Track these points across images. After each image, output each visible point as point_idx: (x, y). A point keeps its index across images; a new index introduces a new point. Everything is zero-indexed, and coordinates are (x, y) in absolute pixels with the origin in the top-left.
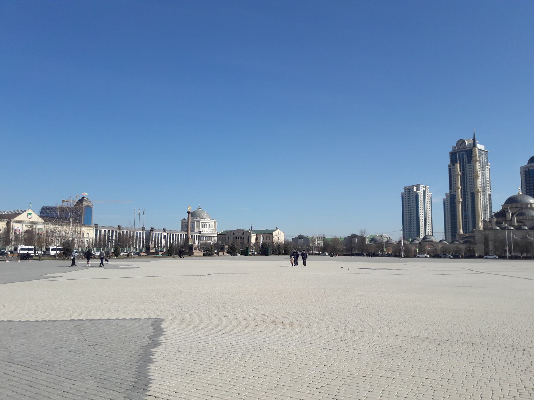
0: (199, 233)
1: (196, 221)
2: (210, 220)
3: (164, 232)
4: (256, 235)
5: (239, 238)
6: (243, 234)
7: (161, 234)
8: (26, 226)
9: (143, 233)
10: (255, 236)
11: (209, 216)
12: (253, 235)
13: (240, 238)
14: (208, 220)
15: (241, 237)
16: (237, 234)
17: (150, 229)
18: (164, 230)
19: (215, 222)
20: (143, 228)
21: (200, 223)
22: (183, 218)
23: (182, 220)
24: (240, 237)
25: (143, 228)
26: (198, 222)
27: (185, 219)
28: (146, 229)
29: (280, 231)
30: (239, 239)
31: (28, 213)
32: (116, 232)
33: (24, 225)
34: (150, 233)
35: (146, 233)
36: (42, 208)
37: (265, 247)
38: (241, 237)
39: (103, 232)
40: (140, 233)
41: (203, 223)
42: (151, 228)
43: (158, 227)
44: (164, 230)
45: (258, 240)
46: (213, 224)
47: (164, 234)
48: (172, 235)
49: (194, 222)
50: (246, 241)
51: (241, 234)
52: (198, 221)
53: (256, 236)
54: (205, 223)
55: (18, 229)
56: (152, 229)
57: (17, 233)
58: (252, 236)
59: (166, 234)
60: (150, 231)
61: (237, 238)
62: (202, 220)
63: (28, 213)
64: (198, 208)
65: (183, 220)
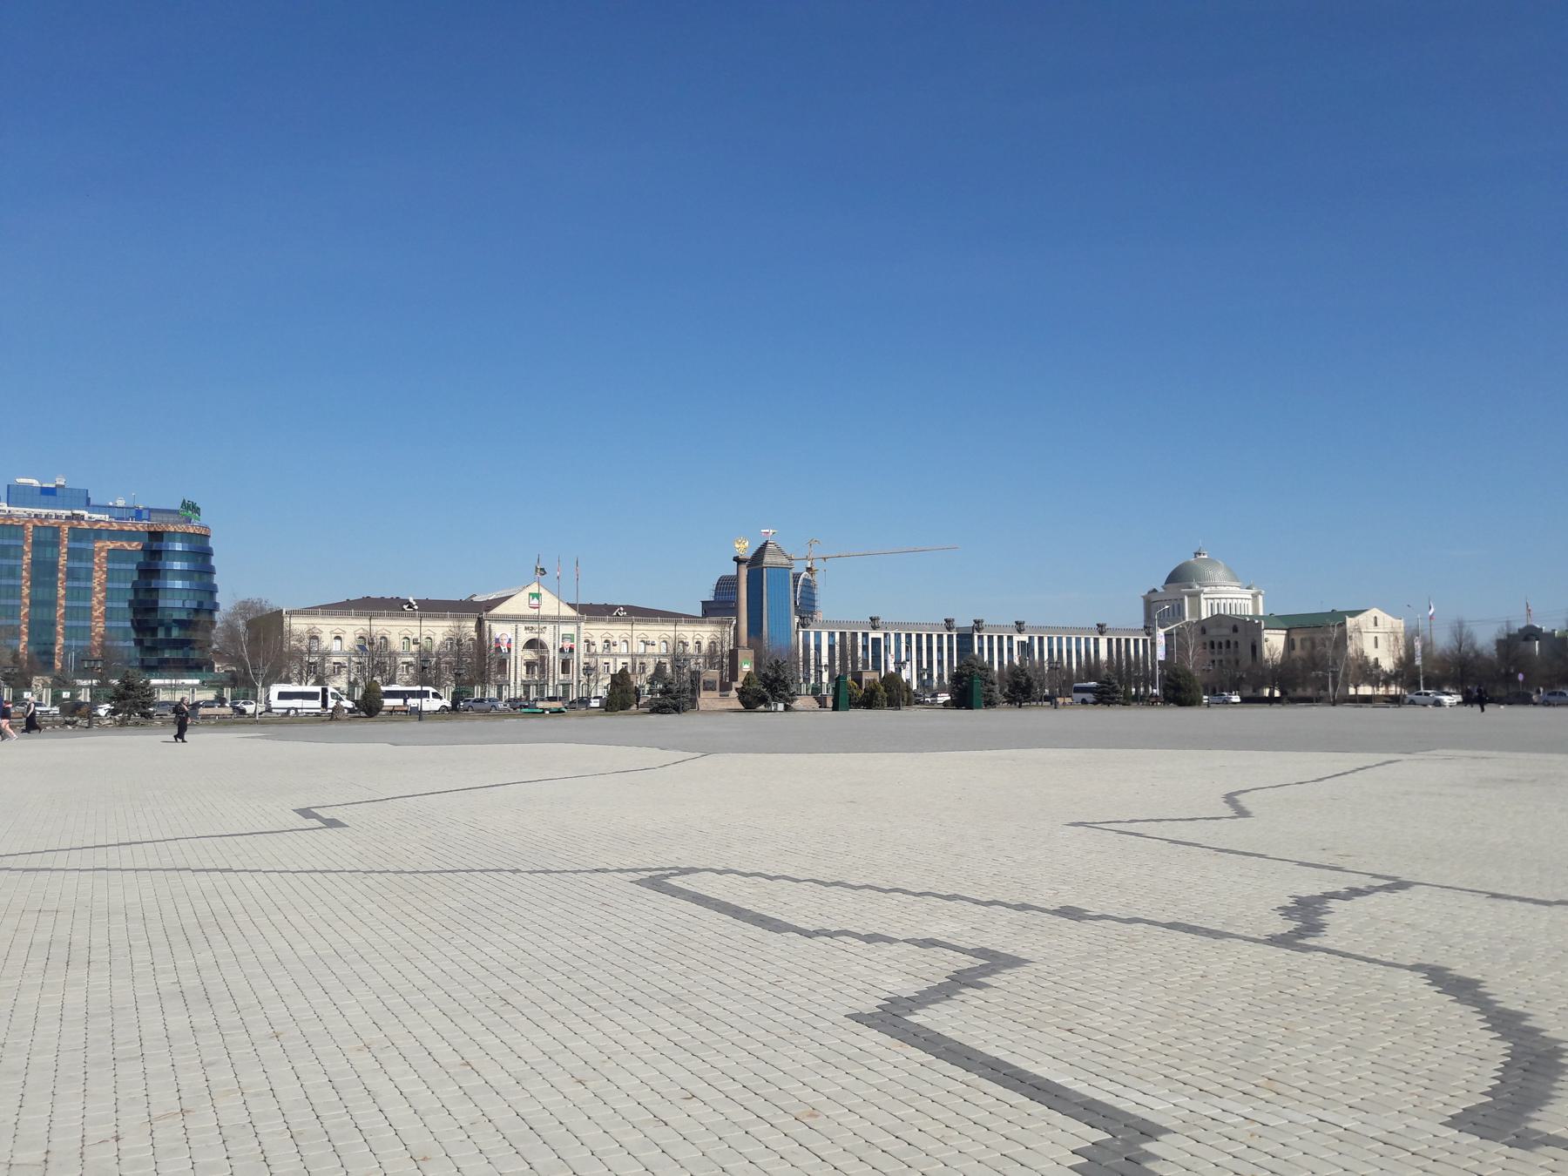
0: (1144, 632)
1: (1189, 596)
2: (1238, 589)
3: (1101, 633)
4: (1285, 632)
5: (1220, 644)
6: (1235, 629)
7: (1010, 638)
8: (526, 628)
9: (950, 637)
10: (1284, 637)
11: (1234, 577)
12: (1268, 631)
13: (1224, 647)
14: (1231, 588)
15: (1228, 643)
16: (1213, 632)
17: (972, 624)
18: (1101, 629)
19: (1255, 596)
20: (949, 624)
21: (1203, 603)
22: (1151, 589)
23: (1145, 593)
24: (1232, 642)
25: (949, 624)
26: (1197, 598)
27: (1155, 591)
28: (957, 624)
29: (1381, 615)
30: (1213, 647)
31: (530, 594)
32: (865, 635)
33: (521, 626)
34: (971, 636)
35: (957, 635)
36: (720, 580)
37: (966, 676)
38: (1228, 643)
39: (825, 636)
40: (940, 637)
41: (1212, 601)
42: (975, 621)
43: (997, 617)
44: (1020, 627)
45: (1294, 648)
46: (1250, 602)
47: (1017, 638)
48: (995, 639)
49: (1183, 600)
50: (1245, 650)
51: (1227, 631)
52: (1195, 596)
53: (1288, 635)
54: (1218, 601)
55: (504, 637)
56: (978, 626)
57: (502, 648)
58: (1266, 636)
59: (1025, 638)
60: (973, 632)
61: (1216, 646)
62: (1206, 590)
63: (530, 594)
64: (1196, 554)
65: (1149, 593)
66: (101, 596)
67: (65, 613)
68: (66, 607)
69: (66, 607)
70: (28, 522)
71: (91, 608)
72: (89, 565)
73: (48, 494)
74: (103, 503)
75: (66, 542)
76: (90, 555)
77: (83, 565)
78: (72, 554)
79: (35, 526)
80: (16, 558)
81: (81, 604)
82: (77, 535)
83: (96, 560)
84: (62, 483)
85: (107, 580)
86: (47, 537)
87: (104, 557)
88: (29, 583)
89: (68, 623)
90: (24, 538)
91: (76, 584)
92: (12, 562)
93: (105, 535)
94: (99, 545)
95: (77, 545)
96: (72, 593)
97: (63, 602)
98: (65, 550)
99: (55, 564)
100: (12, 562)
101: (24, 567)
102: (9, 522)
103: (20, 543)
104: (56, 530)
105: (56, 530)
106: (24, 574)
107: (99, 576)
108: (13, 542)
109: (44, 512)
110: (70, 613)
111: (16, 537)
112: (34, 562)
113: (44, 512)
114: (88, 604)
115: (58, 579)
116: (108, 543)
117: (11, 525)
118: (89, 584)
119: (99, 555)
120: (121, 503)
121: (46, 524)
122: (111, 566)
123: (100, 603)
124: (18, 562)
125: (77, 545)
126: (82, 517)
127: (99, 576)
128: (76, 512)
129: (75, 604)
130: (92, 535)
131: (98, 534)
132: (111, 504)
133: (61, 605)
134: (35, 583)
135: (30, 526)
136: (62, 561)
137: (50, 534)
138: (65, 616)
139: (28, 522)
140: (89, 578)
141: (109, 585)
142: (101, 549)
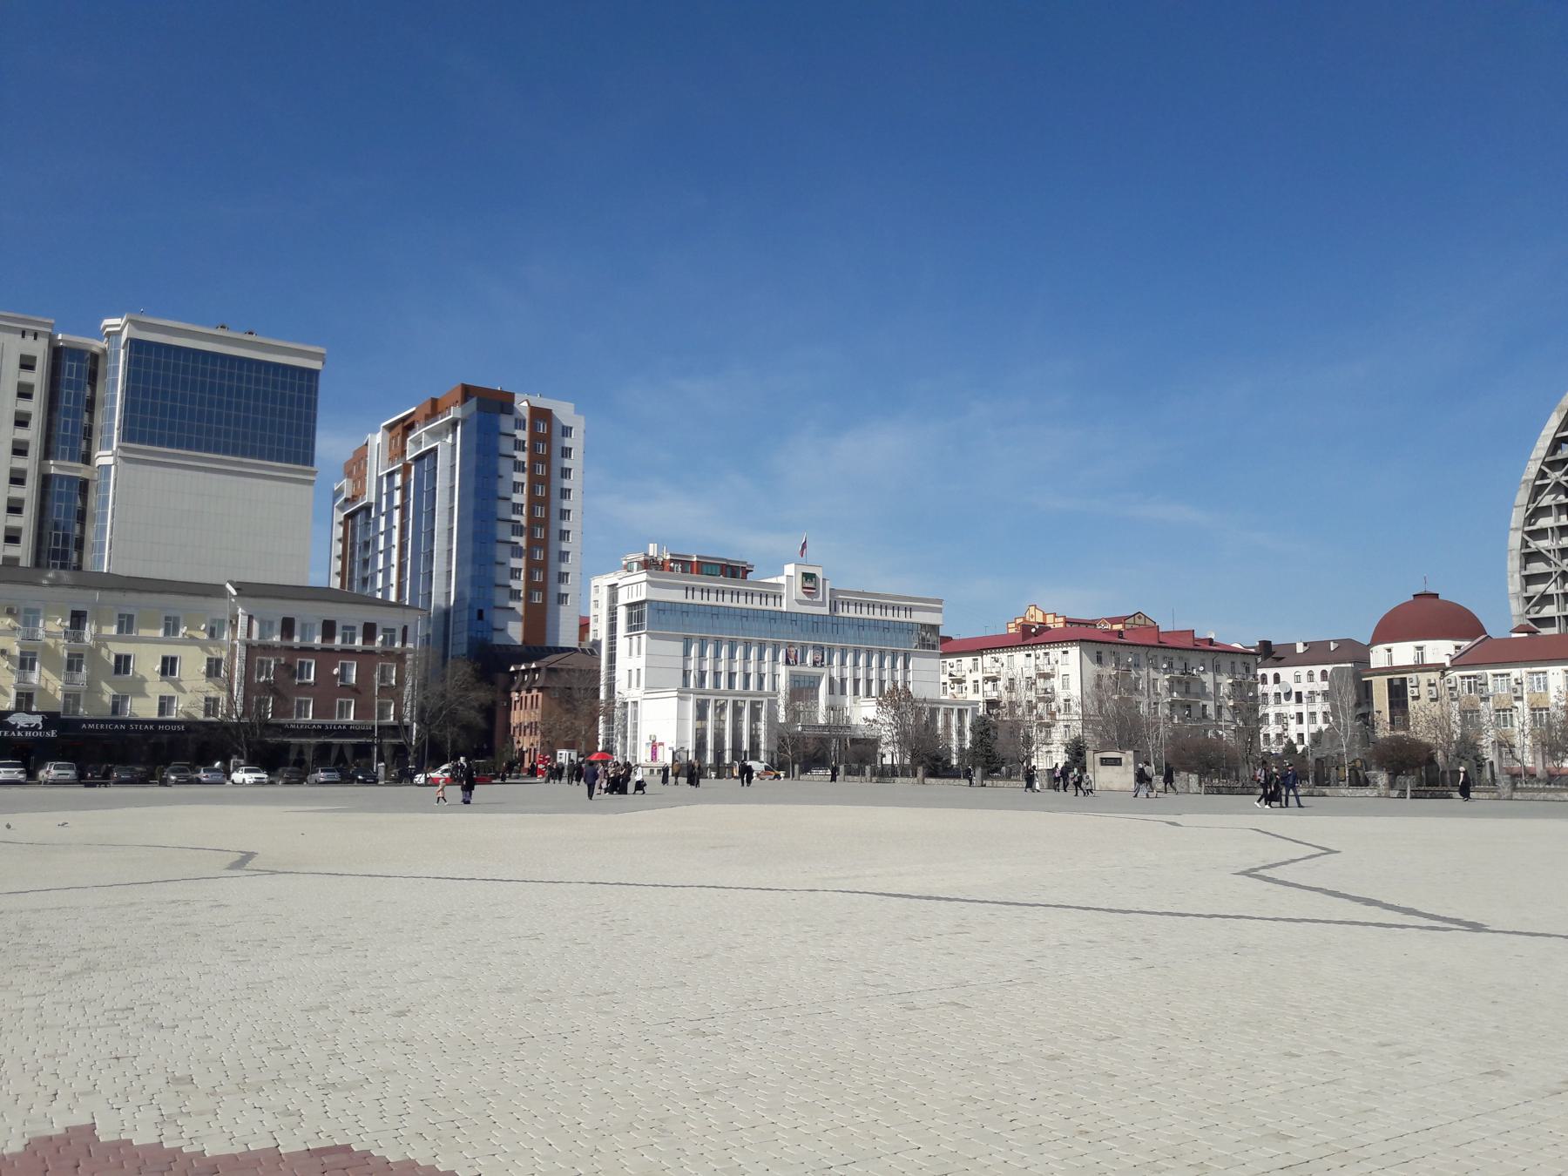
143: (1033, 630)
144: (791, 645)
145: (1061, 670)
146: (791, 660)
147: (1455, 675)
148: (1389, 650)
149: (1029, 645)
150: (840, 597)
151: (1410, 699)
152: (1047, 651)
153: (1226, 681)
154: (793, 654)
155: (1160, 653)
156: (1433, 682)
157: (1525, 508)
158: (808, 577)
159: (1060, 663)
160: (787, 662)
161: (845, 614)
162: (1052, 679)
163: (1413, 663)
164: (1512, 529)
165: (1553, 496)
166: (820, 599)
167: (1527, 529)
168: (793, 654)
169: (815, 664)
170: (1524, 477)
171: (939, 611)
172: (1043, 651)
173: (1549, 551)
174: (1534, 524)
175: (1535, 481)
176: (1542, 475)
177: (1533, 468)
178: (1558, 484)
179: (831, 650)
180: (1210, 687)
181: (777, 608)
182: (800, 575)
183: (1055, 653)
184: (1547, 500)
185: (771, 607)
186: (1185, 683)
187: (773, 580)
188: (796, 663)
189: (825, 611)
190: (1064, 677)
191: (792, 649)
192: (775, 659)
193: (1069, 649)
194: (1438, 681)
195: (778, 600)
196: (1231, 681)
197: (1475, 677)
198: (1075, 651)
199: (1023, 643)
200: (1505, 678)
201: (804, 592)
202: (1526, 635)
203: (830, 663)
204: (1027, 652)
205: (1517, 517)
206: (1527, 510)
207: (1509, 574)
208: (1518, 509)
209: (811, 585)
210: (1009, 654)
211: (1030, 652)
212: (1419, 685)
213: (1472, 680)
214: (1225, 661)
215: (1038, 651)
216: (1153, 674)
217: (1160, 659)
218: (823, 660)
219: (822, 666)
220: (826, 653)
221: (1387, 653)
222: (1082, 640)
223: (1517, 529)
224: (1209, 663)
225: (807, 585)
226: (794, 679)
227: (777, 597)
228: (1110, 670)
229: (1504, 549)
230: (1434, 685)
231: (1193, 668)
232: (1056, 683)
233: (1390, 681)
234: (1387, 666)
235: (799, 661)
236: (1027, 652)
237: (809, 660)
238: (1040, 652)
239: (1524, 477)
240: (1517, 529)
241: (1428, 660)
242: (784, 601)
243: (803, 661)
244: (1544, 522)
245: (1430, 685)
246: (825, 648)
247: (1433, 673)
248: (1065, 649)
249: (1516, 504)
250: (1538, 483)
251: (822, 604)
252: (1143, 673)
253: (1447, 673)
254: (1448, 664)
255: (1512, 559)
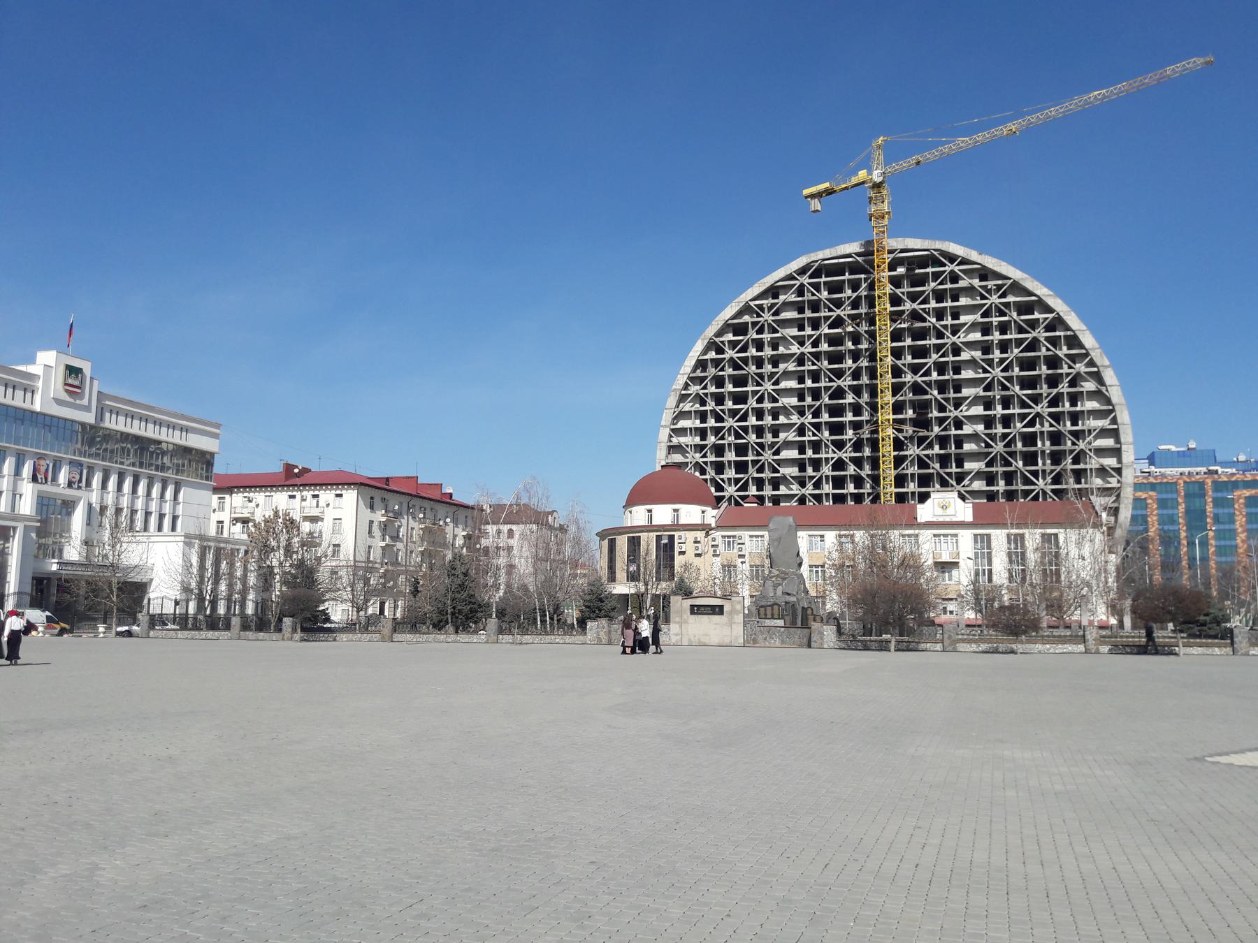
66: (1243, 536)
67: (1215, 551)
68: (1216, 546)
69: (1216, 546)
70: (1179, 479)
71: (1236, 546)
72: (1232, 511)
73: (1187, 457)
74: (1228, 459)
75: (1210, 493)
76: (1231, 503)
77: (1226, 511)
78: (1217, 503)
79: (1185, 482)
80: (1172, 508)
81: (1228, 543)
82: (1219, 486)
83: (1236, 506)
84: (1194, 446)
85: (1248, 522)
86: (1195, 491)
87: (1242, 504)
88: (1185, 528)
89: (1219, 559)
90: (1177, 492)
91: (1222, 527)
92: (1170, 512)
93: (1241, 484)
94: (1237, 493)
95: (1219, 495)
96: (1220, 535)
97: (1212, 542)
98: (1210, 500)
99: (1204, 511)
100: (1170, 512)
101: (1180, 515)
102: (1165, 480)
103: (1175, 496)
104: (1202, 484)
105: (1202, 484)
106: (1181, 520)
107: (1240, 520)
108: (1170, 496)
109: (1186, 470)
110: (1220, 551)
111: (1172, 492)
112: (1187, 512)
113: (1186, 470)
114: (1233, 543)
115: (1207, 523)
116: (1245, 491)
117: (1167, 483)
118: (1232, 527)
119: (1238, 501)
120: (1242, 458)
121: (1193, 479)
122: (1249, 510)
123: (1243, 541)
124: (1175, 511)
125: (1219, 495)
126: (1216, 472)
127: (1240, 520)
128: (1212, 468)
129: (1223, 543)
130: (1230, 487)
131: (1235, 485)
132: (1235, 459)
133: (1212, 544)
134: (1190, 528)
135: (1181, 482)
136: (1209, 508)
137: (1197, 486)
138: (1216, 554)
139: (1179, 479)
140: (1232, 521)
141: (1250, 526)
142: (1239, 497)
143: (296, 471)
144: (41, 457)
145: (329, 515)
146: (39, 477)
147: (718, 535)
148: (650, 511)
149: (296, 485)
150: (108, 403)
151: (676, 553)
152: (316, 493)
153: (461, 533)
154: (43, 469)
155: (417, 502)
156: (699, 540)
157: (673, 411)
158: (72, 371)
159: (331, 506)
160: (35, 479)
161: (113, 426)
162: (320, 523)
163: (700, 522)
164: (662, 426)
165: (691, 404)
166: (85, 402)
167: (673, 427)
168: (43, 469)
169: (70, 484)
170: (674, 387)
171: (216, 436)
172: (312, 493)
173: (687, 446)
174: (676, 424)
175: (681, 390)
176: (686, 386)
177: (681, 380)
178: (697, 394)
179: (91, 470)
180: (449, 537)
181: (27, 406)
182: (62, 368)
183: (327, 496)
184: (687, 407)
185: (18, 402)
186: (433, 535)
187: (22, 368)
188: (46, 482)
189: (90, 418)
190: (336, 521)
191: (42, 462)
192: (17, 473)
193: (344, 492)
194: (703, 538)
195: (29, 395)
196: (465, 533)
197: (734, 537)
198: (351, 496)
199: (287, 483)
200: (760, 539)
201: (67, 391)
202: (756, 505)
203: (88, 484)
204: (290, 493)
205: (667, 417)
206: (674, 412)
207: (657, 461)
208: (668, 411)
209: (76, 383)
210: (268, 494)
211: (294, 493)
212: (685, 541)
213: (731, 539)
214: (462, 513)
215: (305, 493)
216: (412, 523)
217: (417, 508)
218: (80, 481)
219: (79, 488)
220: (85, 472)
221: (647, 514)
222: (362, 484)
223: (665, 426)
224: (461, 518)
225: (70, 381)
226: (43, 502)
227: (29, 390)
228: (380, 516)
229: (656, 442)
230: (699, 542)
231: (440, 520)
232: (326, 526)
233: (659, 538)
234: (647, 524)
235: (49, 479)
236: (290, 493)
237: (63, 477)
238: (308, 494)
239: (674, 387)
240: (665, 426)
241: (683, 521)
242: (38, 397)
243: (55, 479)
244: (683, 423)
245: (696, 542)
246: (85, 466)
247: (699, 532)
248: (339, 492)
249: (667, 407)
250: (683, 392)
251: (87, 409)
252: (404, 522)
253: (710, 532)
254: (713, 525)
255: (661, 449)
